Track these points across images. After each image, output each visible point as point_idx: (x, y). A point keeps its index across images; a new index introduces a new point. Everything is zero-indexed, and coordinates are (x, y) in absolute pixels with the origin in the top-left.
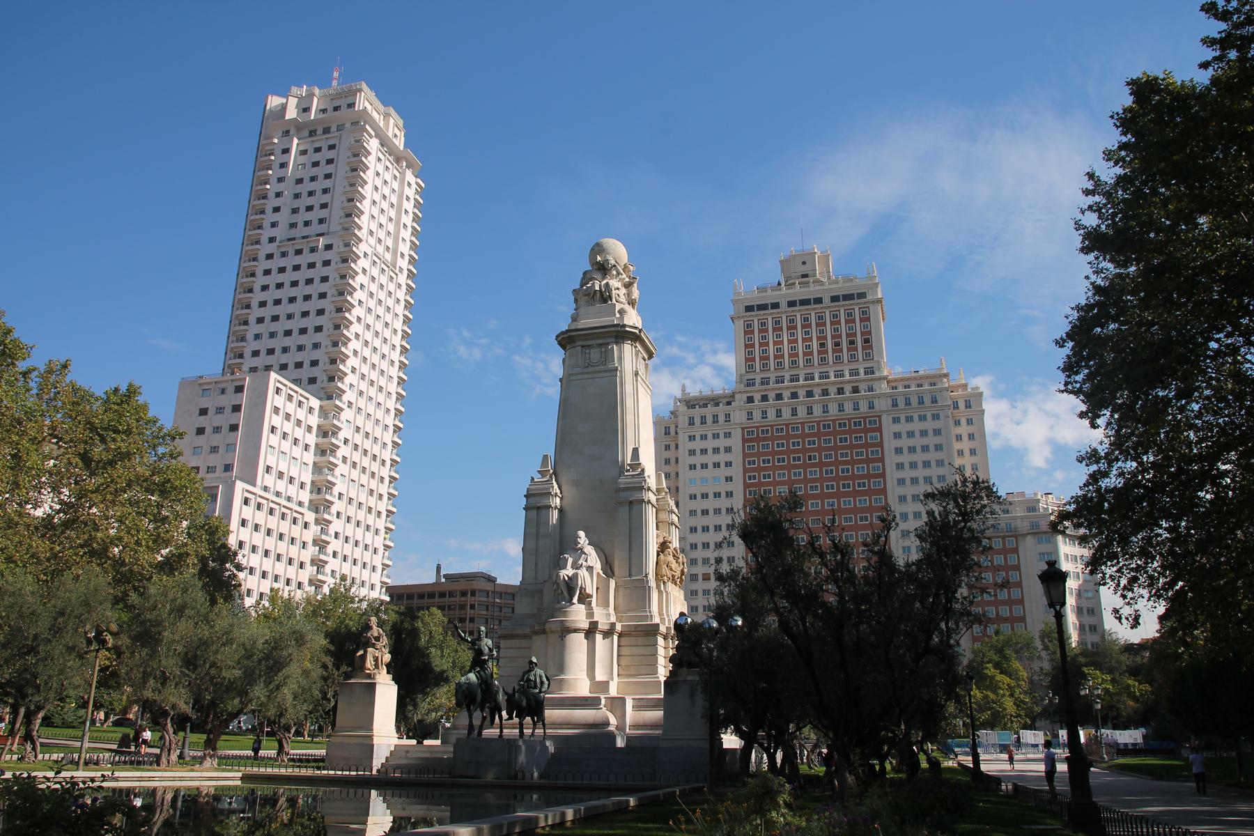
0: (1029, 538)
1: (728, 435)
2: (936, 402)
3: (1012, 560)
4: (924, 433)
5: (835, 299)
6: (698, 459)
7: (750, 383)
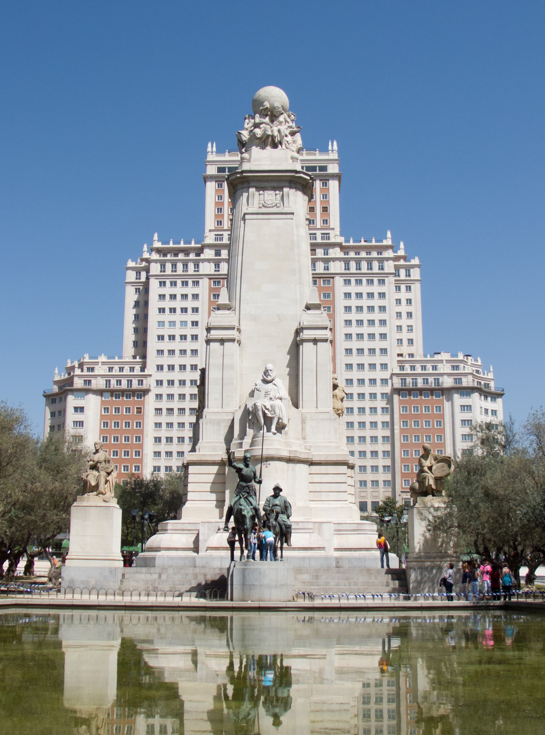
1: (196, 283)
2: (383, 269)
4: (371, 295)
6: (167, 304)
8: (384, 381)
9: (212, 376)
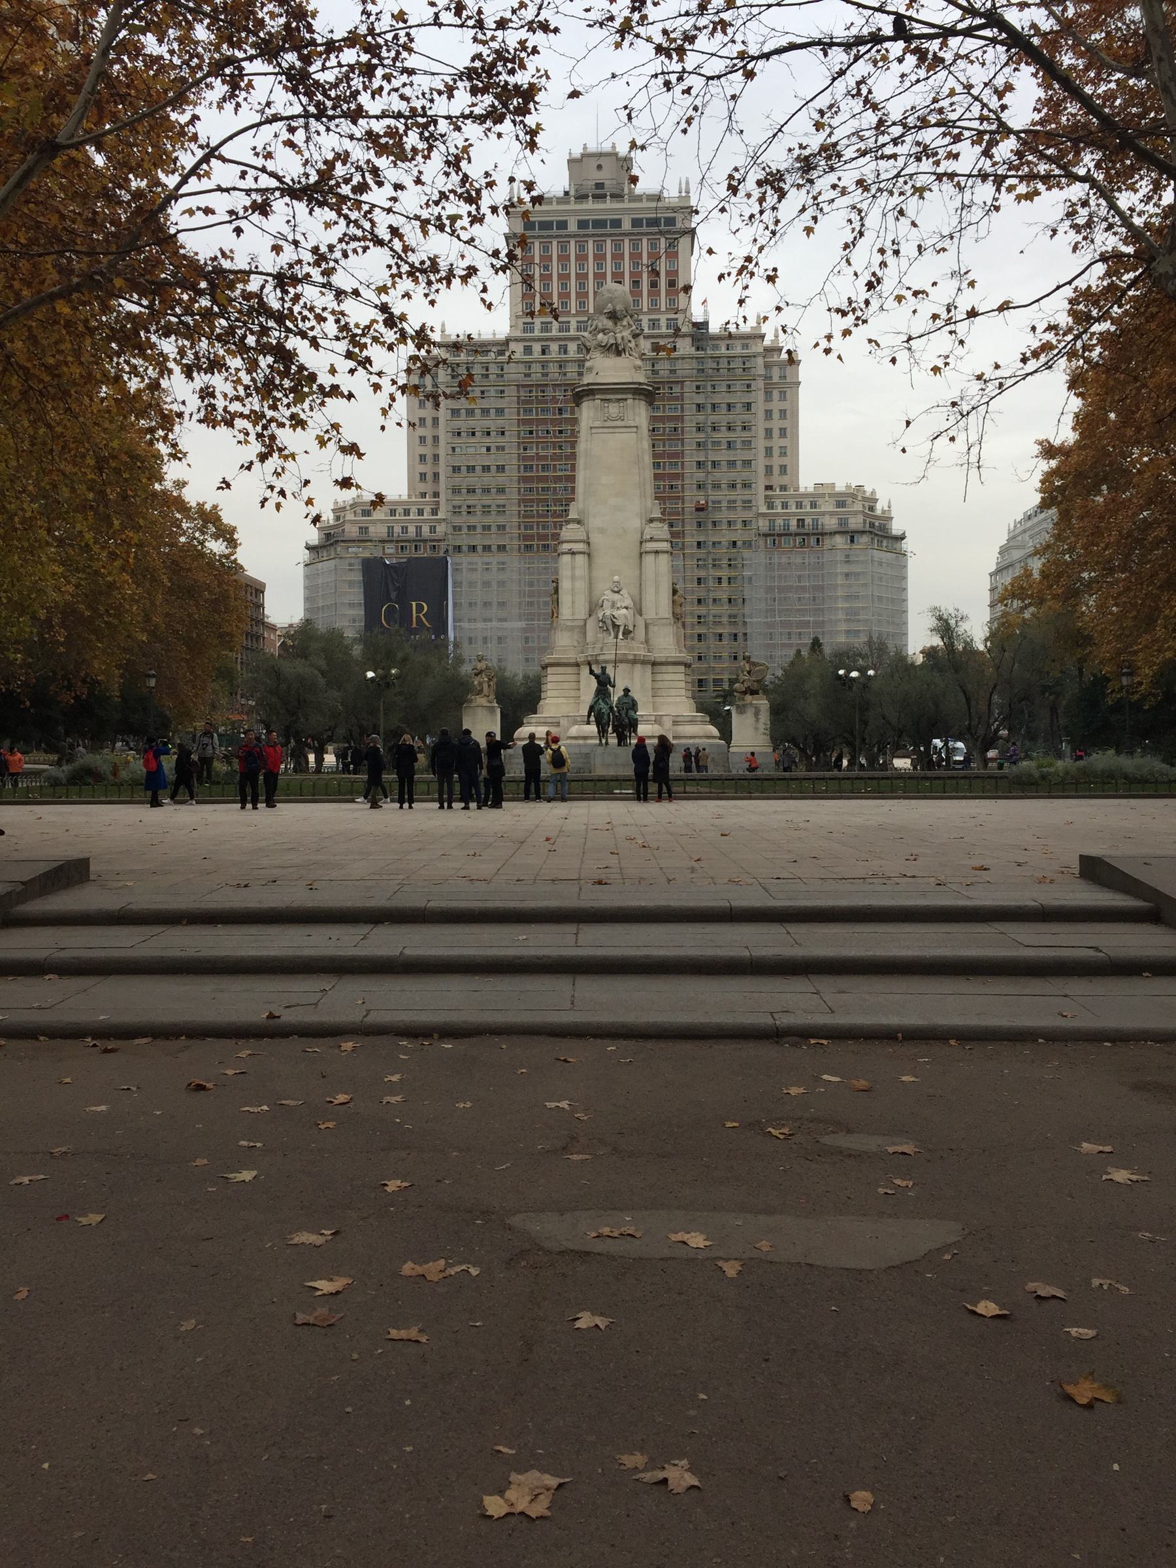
5: (636, 223)
7: (528, 328)
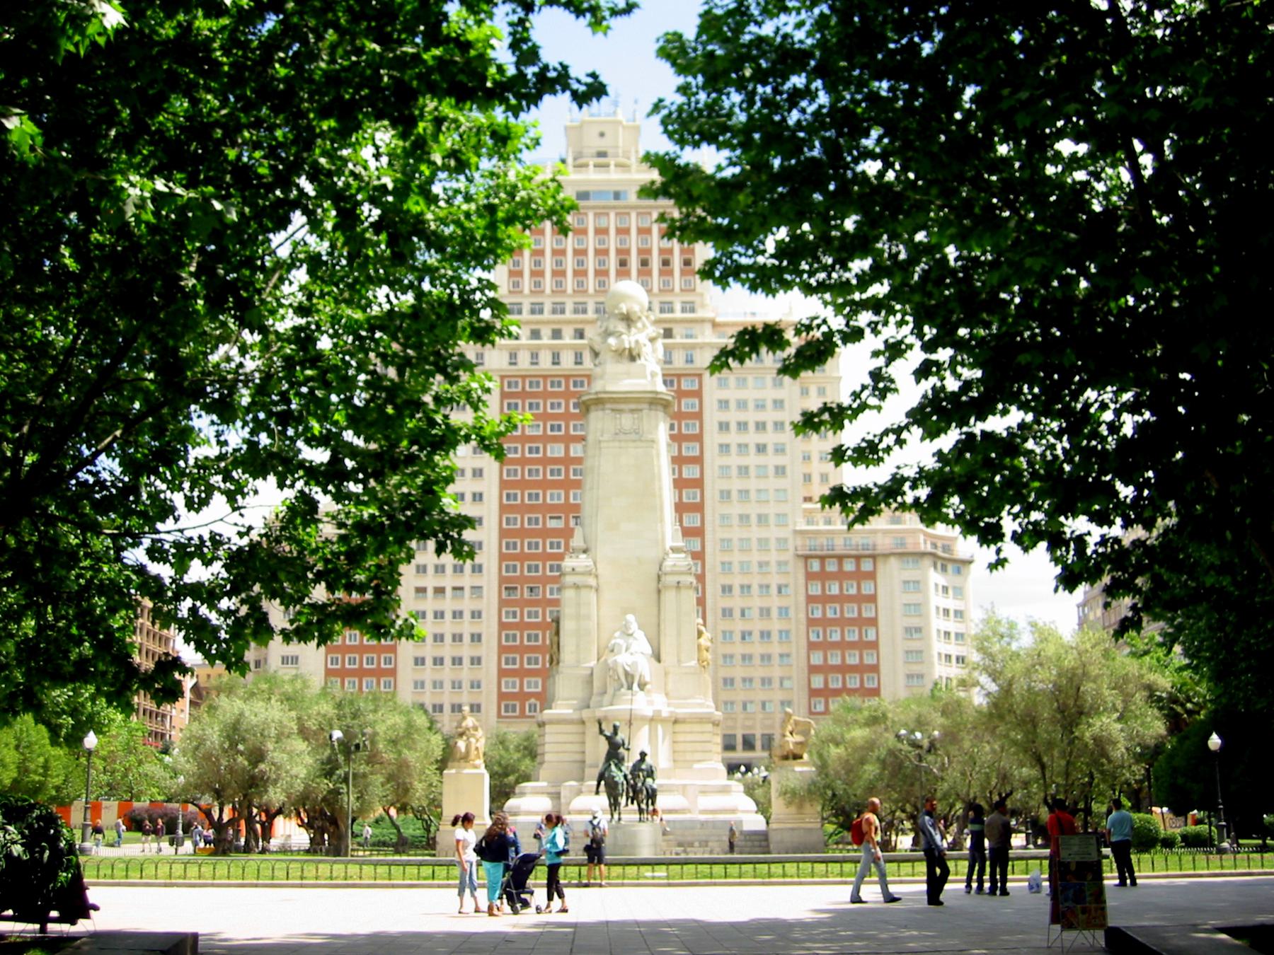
0: (893, 560)
3: (867, 588)
8: (782, 541)
9: (567, 626)
